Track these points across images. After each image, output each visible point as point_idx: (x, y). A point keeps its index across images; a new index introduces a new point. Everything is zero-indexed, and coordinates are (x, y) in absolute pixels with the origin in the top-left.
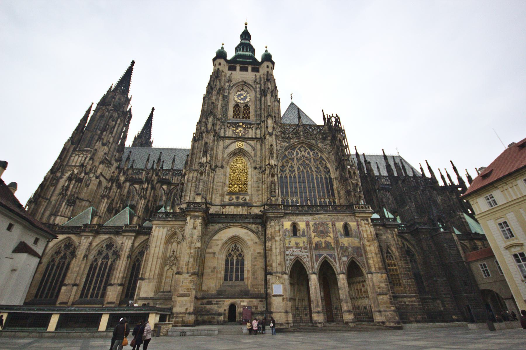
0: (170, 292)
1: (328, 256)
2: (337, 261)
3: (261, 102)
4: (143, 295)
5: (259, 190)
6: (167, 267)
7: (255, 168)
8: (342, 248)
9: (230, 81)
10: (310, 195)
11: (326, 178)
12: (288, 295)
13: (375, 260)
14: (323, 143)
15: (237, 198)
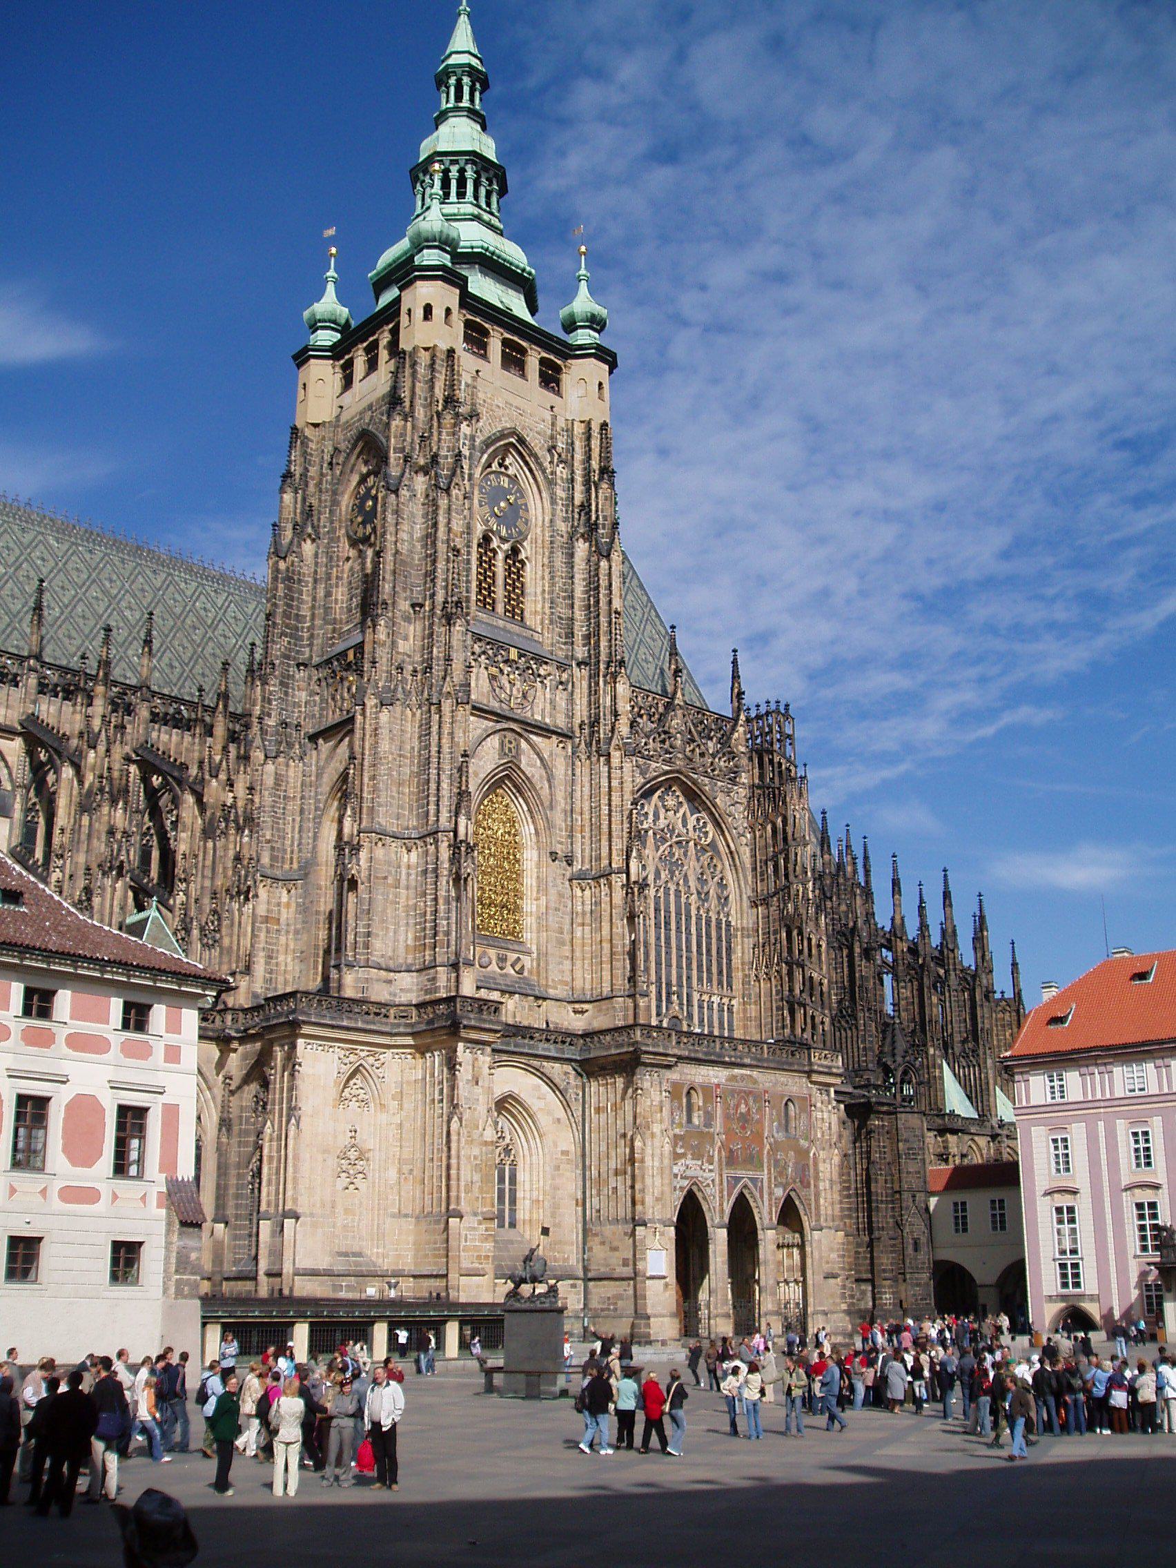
0: (360, 1255)
1: (750, 1185)
2: (766, 1196)
3: (571, 565)
4: (304, 1263)
5: (561, 943)
6: (344, 1180)
7: (554, 856)
8: (777, 1161)
9: (473, 416)
10: (680, 977)
11: (719, 922)
12: (672, 1279)
13: (829, 1196)
14: (728, 794)
15: (502, 960)
